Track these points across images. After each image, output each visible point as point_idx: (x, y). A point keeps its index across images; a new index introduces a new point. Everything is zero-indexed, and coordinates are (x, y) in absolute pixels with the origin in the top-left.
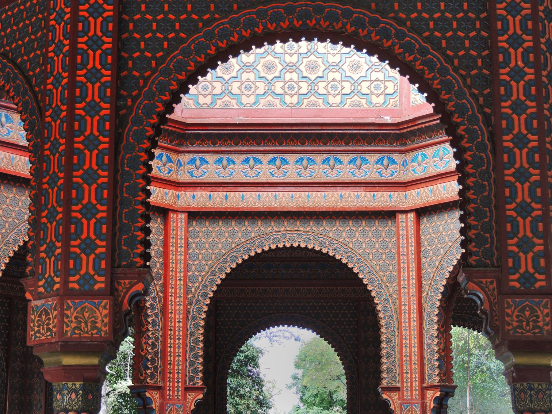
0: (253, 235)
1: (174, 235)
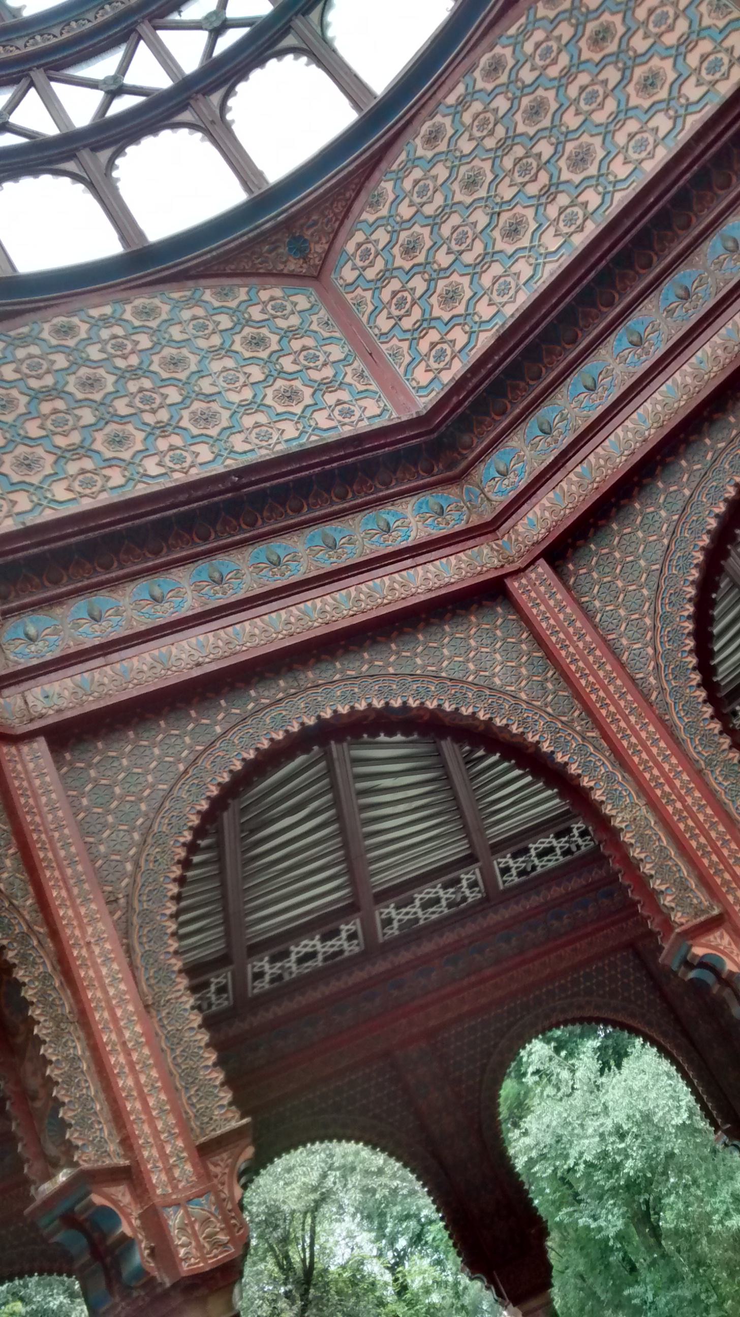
0: (687, 492)
1: (544, 613)
